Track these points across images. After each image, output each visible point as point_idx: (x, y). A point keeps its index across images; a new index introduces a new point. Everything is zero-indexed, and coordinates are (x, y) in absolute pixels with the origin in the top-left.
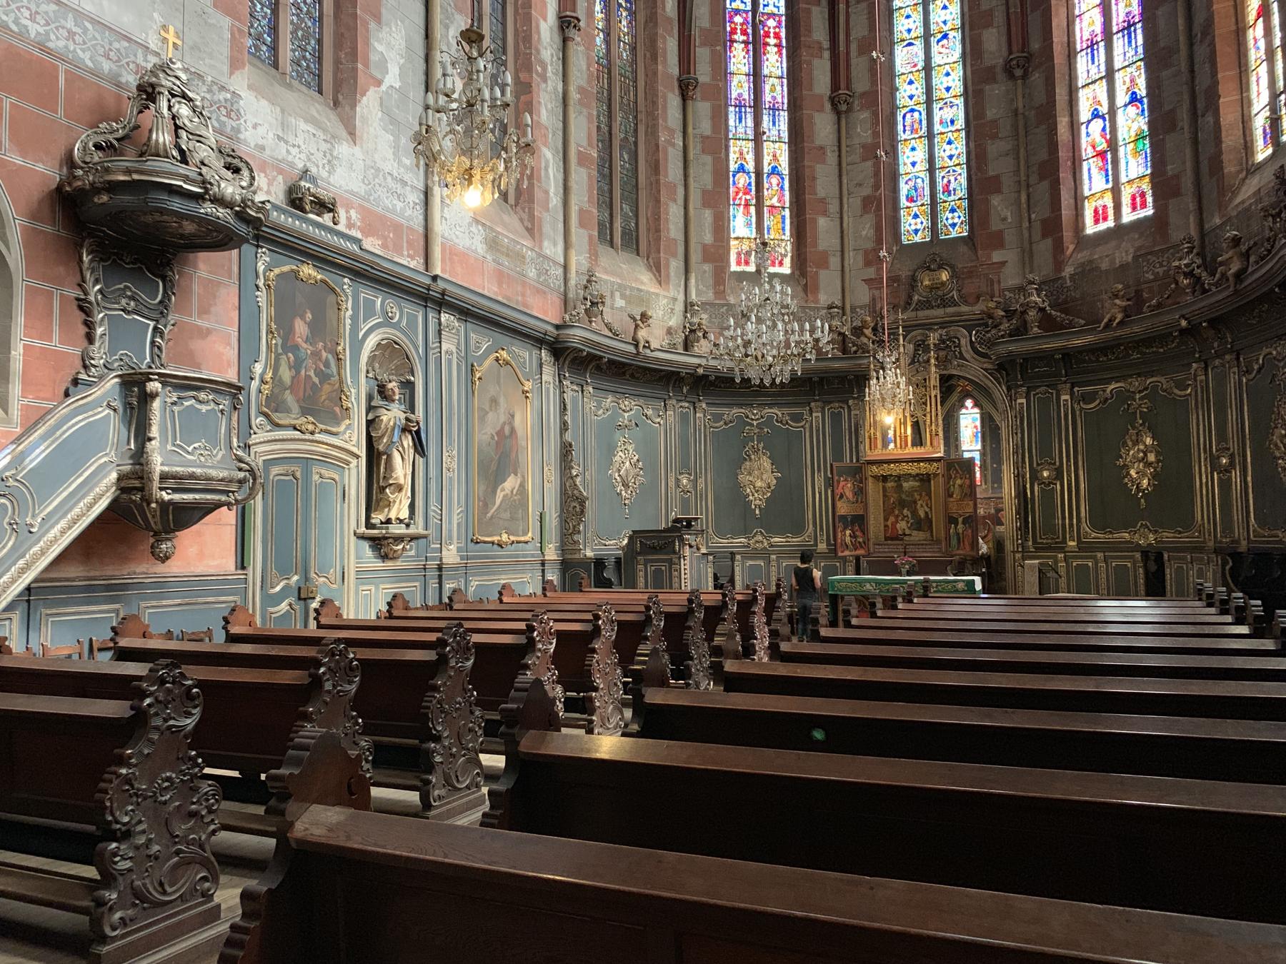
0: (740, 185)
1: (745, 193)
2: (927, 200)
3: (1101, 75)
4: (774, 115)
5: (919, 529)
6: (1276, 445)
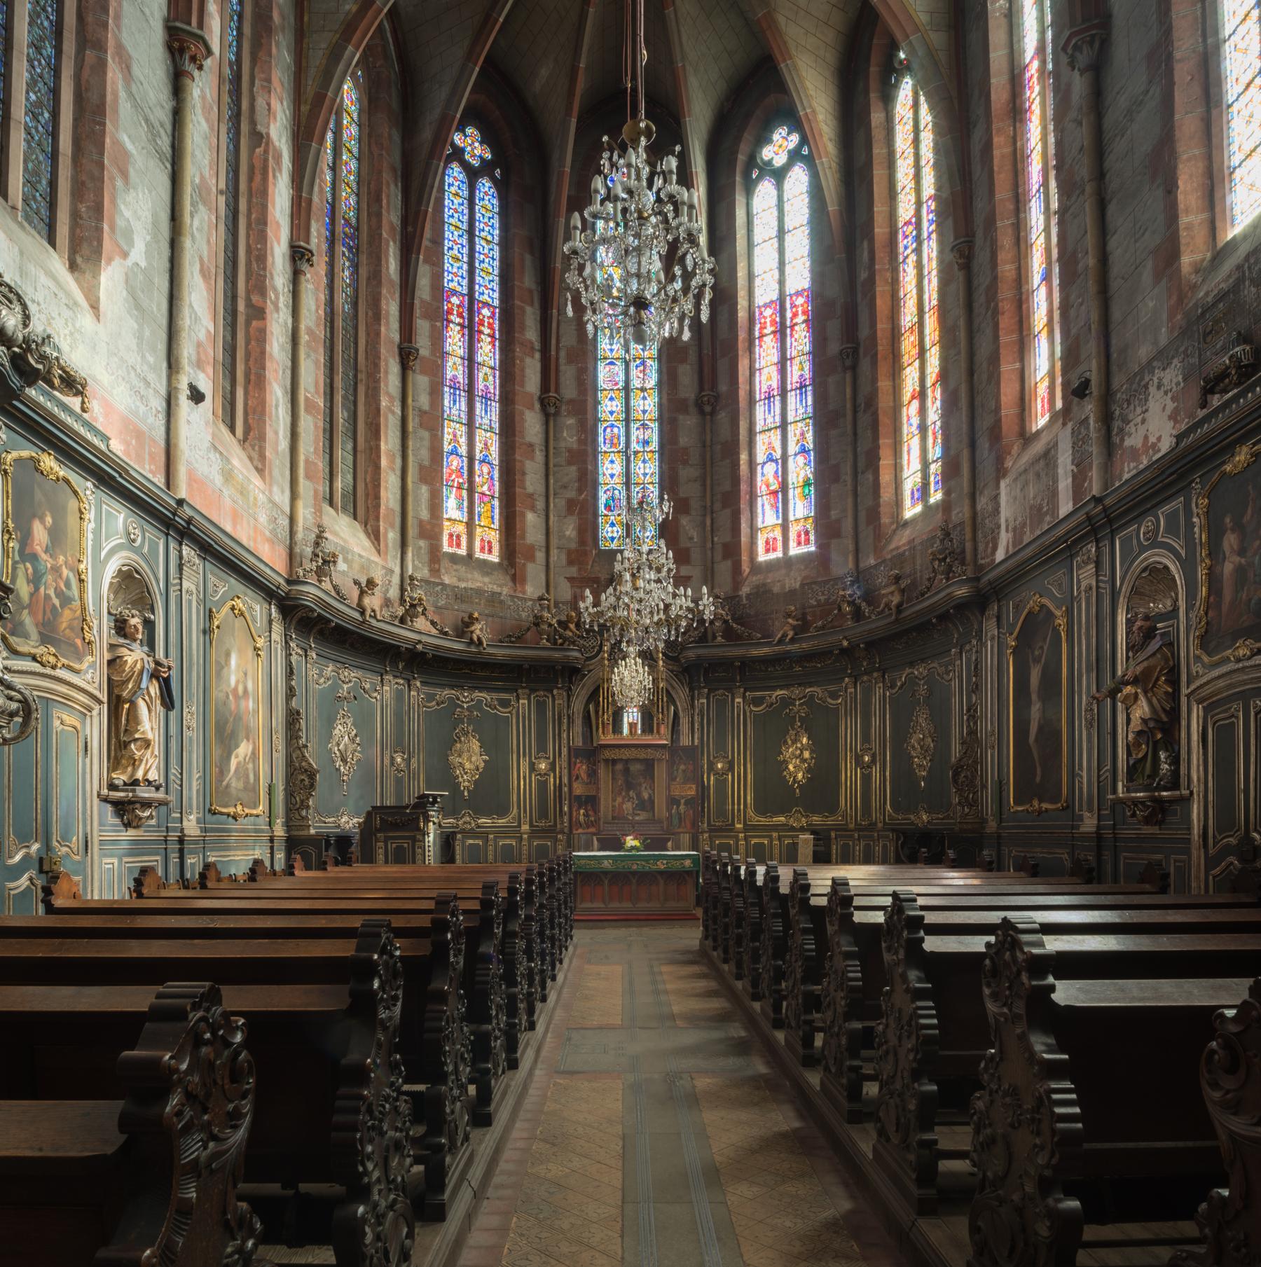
0: (453, 468)
1: (457, 477)
5: (643, 809)
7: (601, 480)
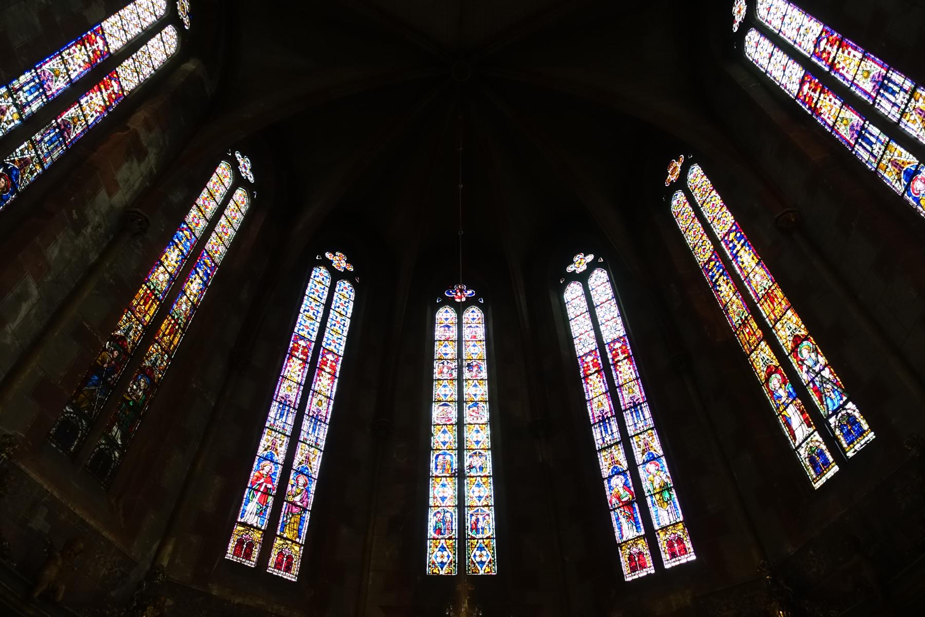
0: (264, 472)
1: (265, 481)
2: (455, 534)
3: (615, 441)
4: (316, 424)
7: (431, 503)
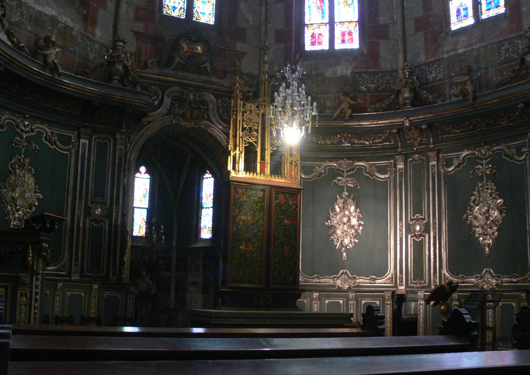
6: (476, 218)
